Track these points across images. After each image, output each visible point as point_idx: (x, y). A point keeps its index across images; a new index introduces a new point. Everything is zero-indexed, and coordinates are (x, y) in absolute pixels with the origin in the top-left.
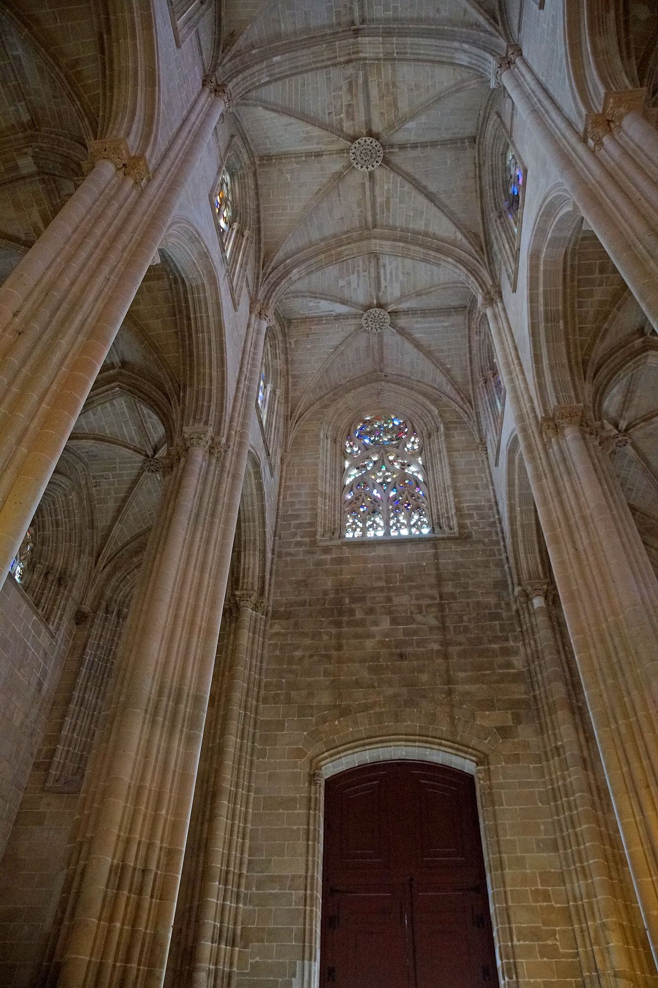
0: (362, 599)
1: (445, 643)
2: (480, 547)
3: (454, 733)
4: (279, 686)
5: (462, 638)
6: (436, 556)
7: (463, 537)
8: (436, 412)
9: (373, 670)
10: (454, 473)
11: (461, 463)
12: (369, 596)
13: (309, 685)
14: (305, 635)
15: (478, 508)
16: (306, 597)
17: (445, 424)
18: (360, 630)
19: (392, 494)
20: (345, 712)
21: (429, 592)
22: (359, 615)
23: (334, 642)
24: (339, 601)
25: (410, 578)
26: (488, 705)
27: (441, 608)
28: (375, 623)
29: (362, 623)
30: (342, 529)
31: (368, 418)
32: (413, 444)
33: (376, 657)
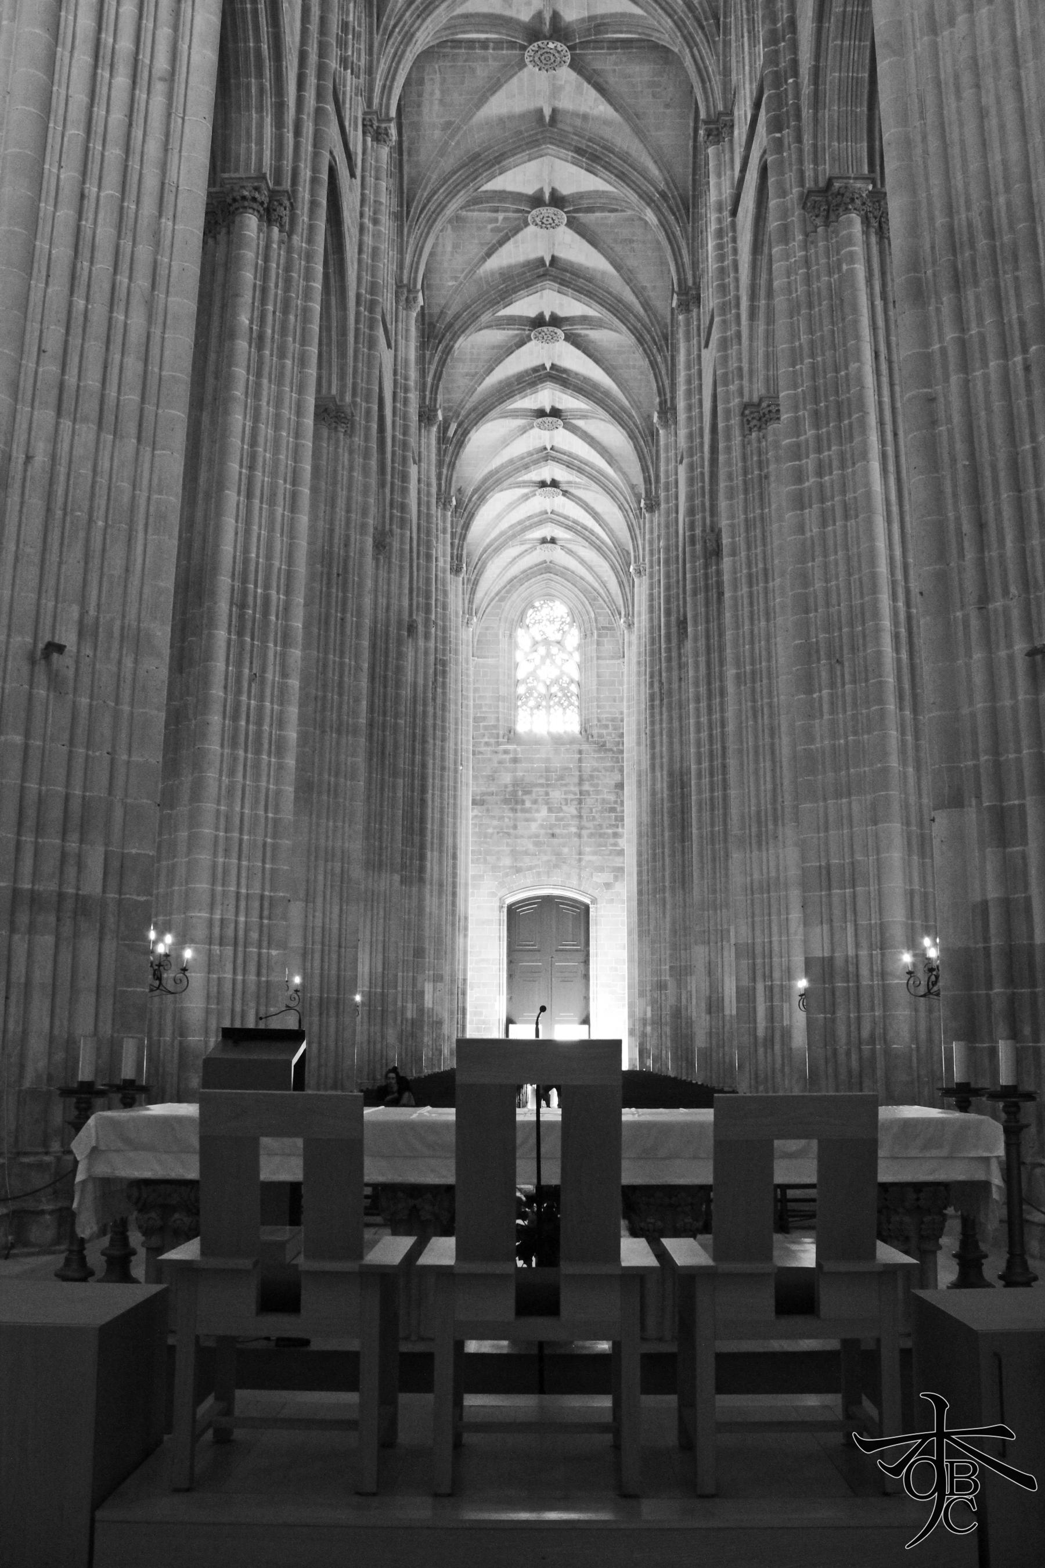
0: (529, 793)
1: (581, 828)
2: (610, 754)
3: (580, 885)
4: (480, 853)
5: (590, 825)
6: (580, 760)
8: (593, 615)
9: (537, 844)
10: (599, 684)
12: (535, 790)
13: (498, 852)
14: (493, 817)
15: (613, 720)
16: (493, 789)
17: (598, 629)
18: (527, 815)
20: (518, 870)
21: (572, 788)
22: (528, 805)
23: (511, 823)
24: (514, 793)
25: (561, 778)
26: (601, 869)
27: (580, 802)
28: (538, 811)
31: (537, 604)
33: (537, 836)
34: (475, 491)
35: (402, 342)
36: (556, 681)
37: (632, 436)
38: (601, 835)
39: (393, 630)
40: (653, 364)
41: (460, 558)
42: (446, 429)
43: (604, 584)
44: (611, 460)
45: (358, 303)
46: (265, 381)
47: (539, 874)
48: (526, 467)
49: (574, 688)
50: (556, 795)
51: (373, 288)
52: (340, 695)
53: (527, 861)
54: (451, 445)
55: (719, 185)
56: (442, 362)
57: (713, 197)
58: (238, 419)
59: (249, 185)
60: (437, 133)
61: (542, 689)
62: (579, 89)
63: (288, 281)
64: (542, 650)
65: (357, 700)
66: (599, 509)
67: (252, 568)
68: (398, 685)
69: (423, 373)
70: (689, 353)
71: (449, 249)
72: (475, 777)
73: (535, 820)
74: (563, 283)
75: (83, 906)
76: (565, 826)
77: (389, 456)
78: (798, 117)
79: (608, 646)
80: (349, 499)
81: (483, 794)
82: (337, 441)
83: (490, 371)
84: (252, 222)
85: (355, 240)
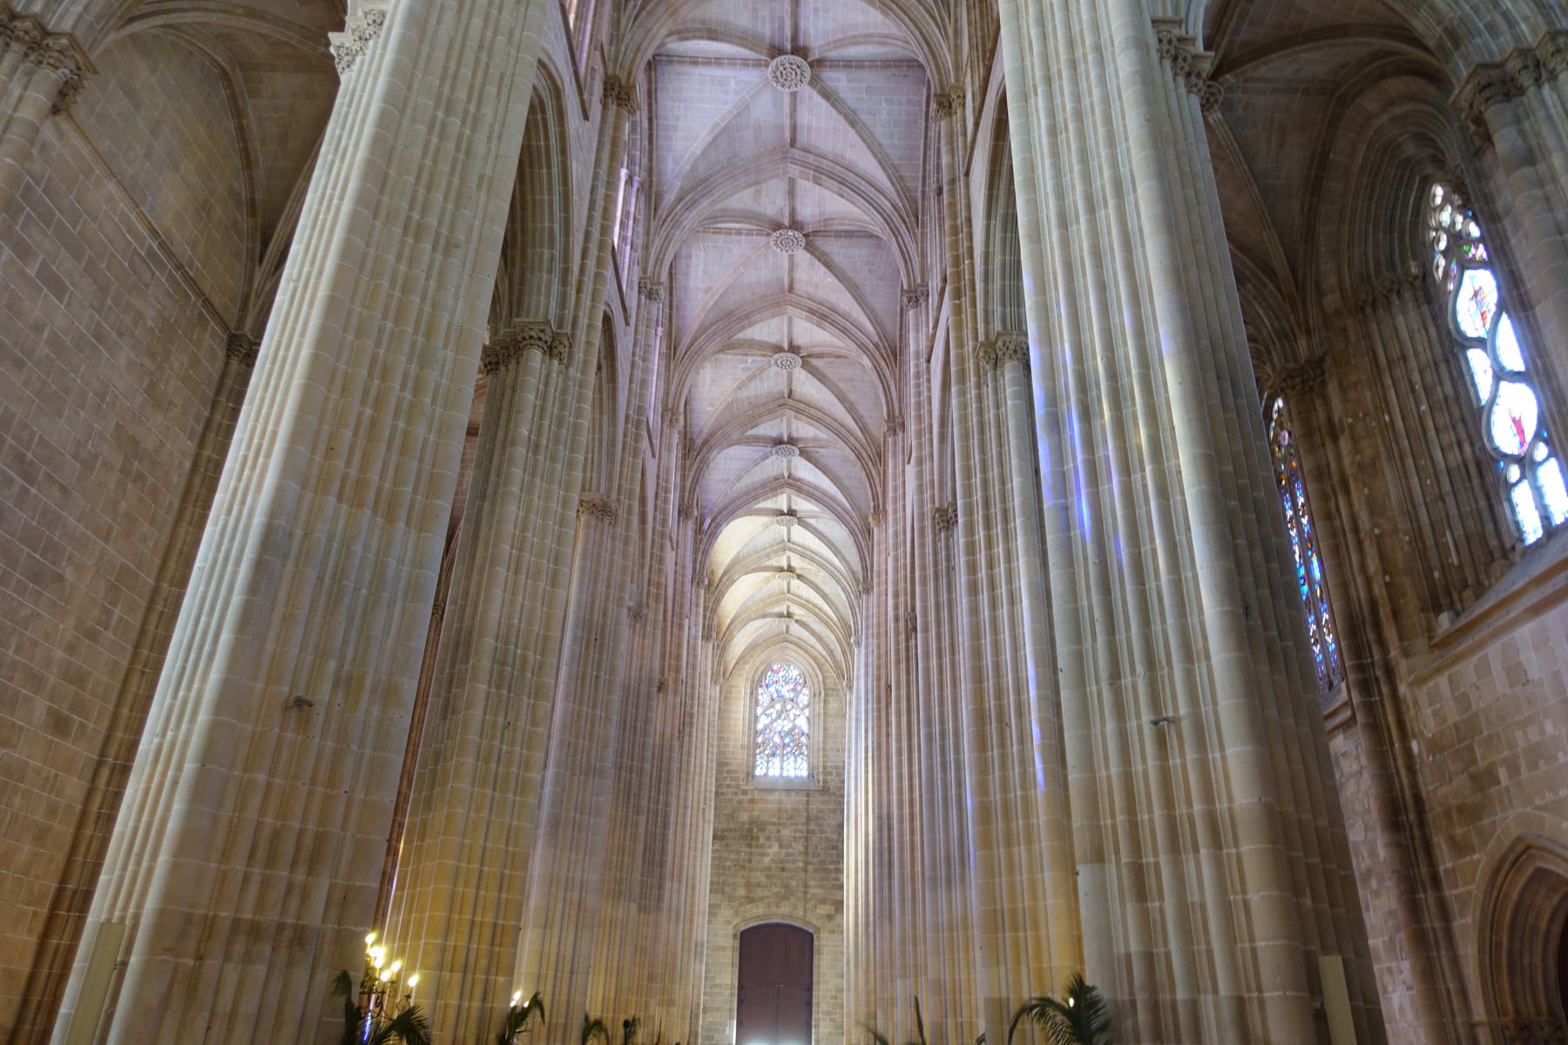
0: (763, 830)
1: (807, 863)
6: (808, 802)
7: (825, 790)
9: (768, 877)
10: (825, 736)
11: (832, 726)
15: (837, 767)
16: (732, 826)
19: (787, 740)
20: (751, 900)
22: (762, 841)
24: (750, 830)
25: (791, 818)
26: (823, 901)
27: (807, 839)
29: (762, 846)
30: (754, 768)
32: (804, 699)
33: (769, 869)
34: (725, 573)
35: (665, 454)
36: (790, 733)
37: (852, 532)
38: (825, 871)
39: (644, 688)
40: (869, 476)
41: (710, 629)
42: (702, 523)
43: (831, 652)
44: (837, 552)
45: (626, 422)
46: (538, 481)
47: (769, 905)
48: (768, 556)
49: (803, 739)
50: (786, 833)
51: (640, 410)
52: (590, 741)
53: (759, 892)
54: (705, 535)
55: (917, 340)
56: (699, 471)
57: (912, 348)
58: (512, 509)
59: (536, 328)
60: (700, 295)
61: (777, 739)
62: (812, 265)
63: (563, 403)
64: (778, 706)
65: (605, 746)
66: (827, 590)
67: (514, 632)
68: (645, 734)
69: (684, 477)
70: (895, 468)
71: (708, 382)
72: (716, 815)
73: (766, 855)
74: (798, 411)
75: (300, 937)
76: (794, 862)
77: (649, 543)
78: (973, 289)
79: (833, 705)
80: (609, 580)
81: (724, 830)
82: (602, 530)
83: (739, 479)
84: (536, 357)
85: (628, 372)
